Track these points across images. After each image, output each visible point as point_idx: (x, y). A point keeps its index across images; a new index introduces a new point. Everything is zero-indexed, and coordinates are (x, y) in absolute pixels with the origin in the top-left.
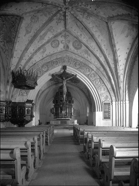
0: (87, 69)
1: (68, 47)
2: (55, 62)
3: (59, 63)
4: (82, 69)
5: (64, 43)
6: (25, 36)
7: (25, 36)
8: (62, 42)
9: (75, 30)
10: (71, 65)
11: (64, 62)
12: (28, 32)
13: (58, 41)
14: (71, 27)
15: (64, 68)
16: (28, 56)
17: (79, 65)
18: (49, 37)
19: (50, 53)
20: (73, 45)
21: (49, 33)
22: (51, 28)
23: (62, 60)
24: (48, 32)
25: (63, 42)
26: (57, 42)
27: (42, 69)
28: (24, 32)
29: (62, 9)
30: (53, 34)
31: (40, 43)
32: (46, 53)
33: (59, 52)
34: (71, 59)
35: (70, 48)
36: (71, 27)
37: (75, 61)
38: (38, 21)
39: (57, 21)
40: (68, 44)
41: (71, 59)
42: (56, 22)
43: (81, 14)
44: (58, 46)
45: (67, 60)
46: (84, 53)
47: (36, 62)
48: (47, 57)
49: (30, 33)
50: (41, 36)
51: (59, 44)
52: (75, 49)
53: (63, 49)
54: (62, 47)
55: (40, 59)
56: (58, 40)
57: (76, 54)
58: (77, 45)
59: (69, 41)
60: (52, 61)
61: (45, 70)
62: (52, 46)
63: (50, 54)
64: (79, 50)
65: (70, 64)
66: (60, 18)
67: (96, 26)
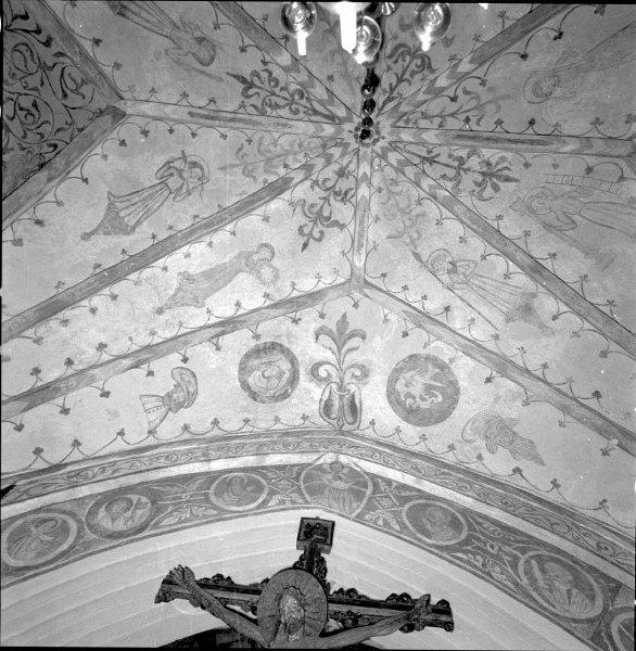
0: (550, 566)
1: (354, 409)
2: (237, 488)
3: (272, 493)
4: (497, 558)
5: (327, 380)
6: (86, 236)
7: (86, 236)
8: (314, 372)
9: (405, 288)
10: (381, 514)
11: (316, 491)
12: (113, 223)
13: (293, 361)
14: (384, 275)
15: (315, 536)
16: (36, 371)
17: (455, 524)
18: (238, 304)
19: (215, 422)
20: (392, 395)
21: (244, 280)
22: (265, 253)
23: (304, 481)
24: (238, 271)
25: (322, 372)
26: (286, 366)
27: (92, 513)
28: (94, 216)
29: (339, 131)
30: (267, 296)
31: (168, 324)
32: (185, 415)
33: (287, 434)
34: (376, 485)
35: (366, 417)
36: (384, 275)
37: (408, 499)
38: (196, 194)
39: (304, 220)
40: (353, 388)
41: (376, 485)
42: (301, 229)
43: (444, 176)
44: (285, 395)
45: (340, 485)
46: (481, 443)
47: (76, 456)
48: (185, 442)
49: (128, 233)
50: (189, 278)
51: (294, 380)
52: (404, 425)
53: (320, 421)
54: (314, 408)
55: (120, 445)
56: (296, 350)
57: (413, 454)
58: (417, 390)
59: (365, 373)
60: (211, 477)
61: (120, 526)
62: (248, 356)
63: (216, 432)
64: (433, 430)
65: (370, 507)
66: (326, 214)
67: (548, 227)
